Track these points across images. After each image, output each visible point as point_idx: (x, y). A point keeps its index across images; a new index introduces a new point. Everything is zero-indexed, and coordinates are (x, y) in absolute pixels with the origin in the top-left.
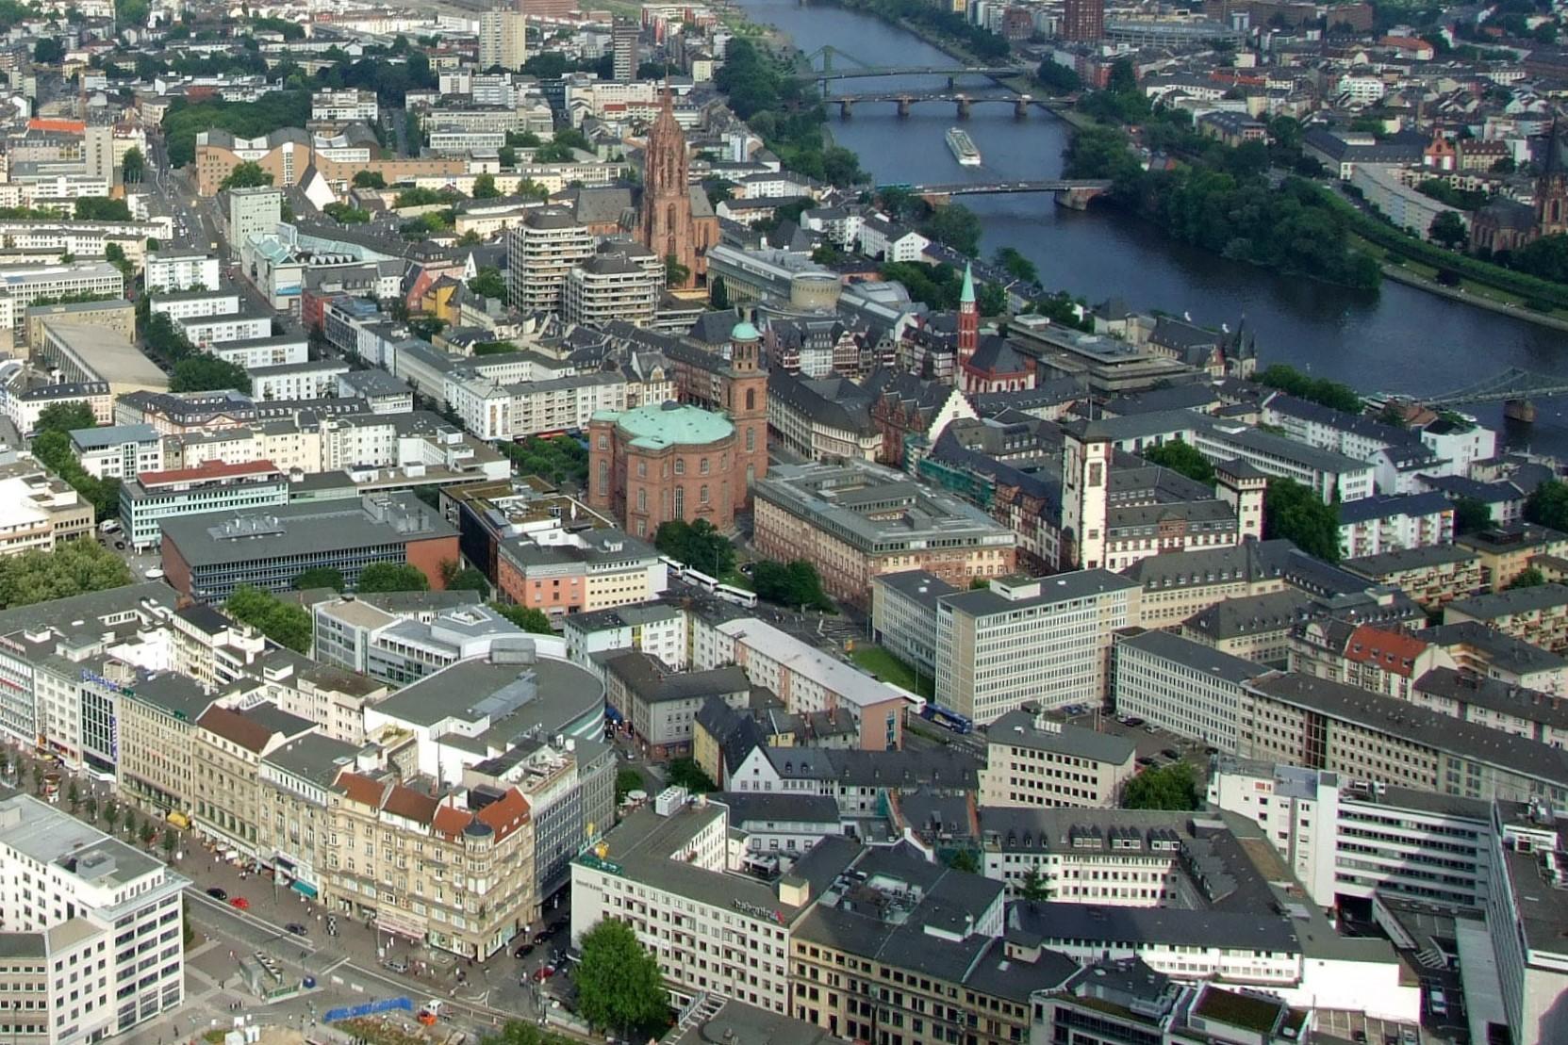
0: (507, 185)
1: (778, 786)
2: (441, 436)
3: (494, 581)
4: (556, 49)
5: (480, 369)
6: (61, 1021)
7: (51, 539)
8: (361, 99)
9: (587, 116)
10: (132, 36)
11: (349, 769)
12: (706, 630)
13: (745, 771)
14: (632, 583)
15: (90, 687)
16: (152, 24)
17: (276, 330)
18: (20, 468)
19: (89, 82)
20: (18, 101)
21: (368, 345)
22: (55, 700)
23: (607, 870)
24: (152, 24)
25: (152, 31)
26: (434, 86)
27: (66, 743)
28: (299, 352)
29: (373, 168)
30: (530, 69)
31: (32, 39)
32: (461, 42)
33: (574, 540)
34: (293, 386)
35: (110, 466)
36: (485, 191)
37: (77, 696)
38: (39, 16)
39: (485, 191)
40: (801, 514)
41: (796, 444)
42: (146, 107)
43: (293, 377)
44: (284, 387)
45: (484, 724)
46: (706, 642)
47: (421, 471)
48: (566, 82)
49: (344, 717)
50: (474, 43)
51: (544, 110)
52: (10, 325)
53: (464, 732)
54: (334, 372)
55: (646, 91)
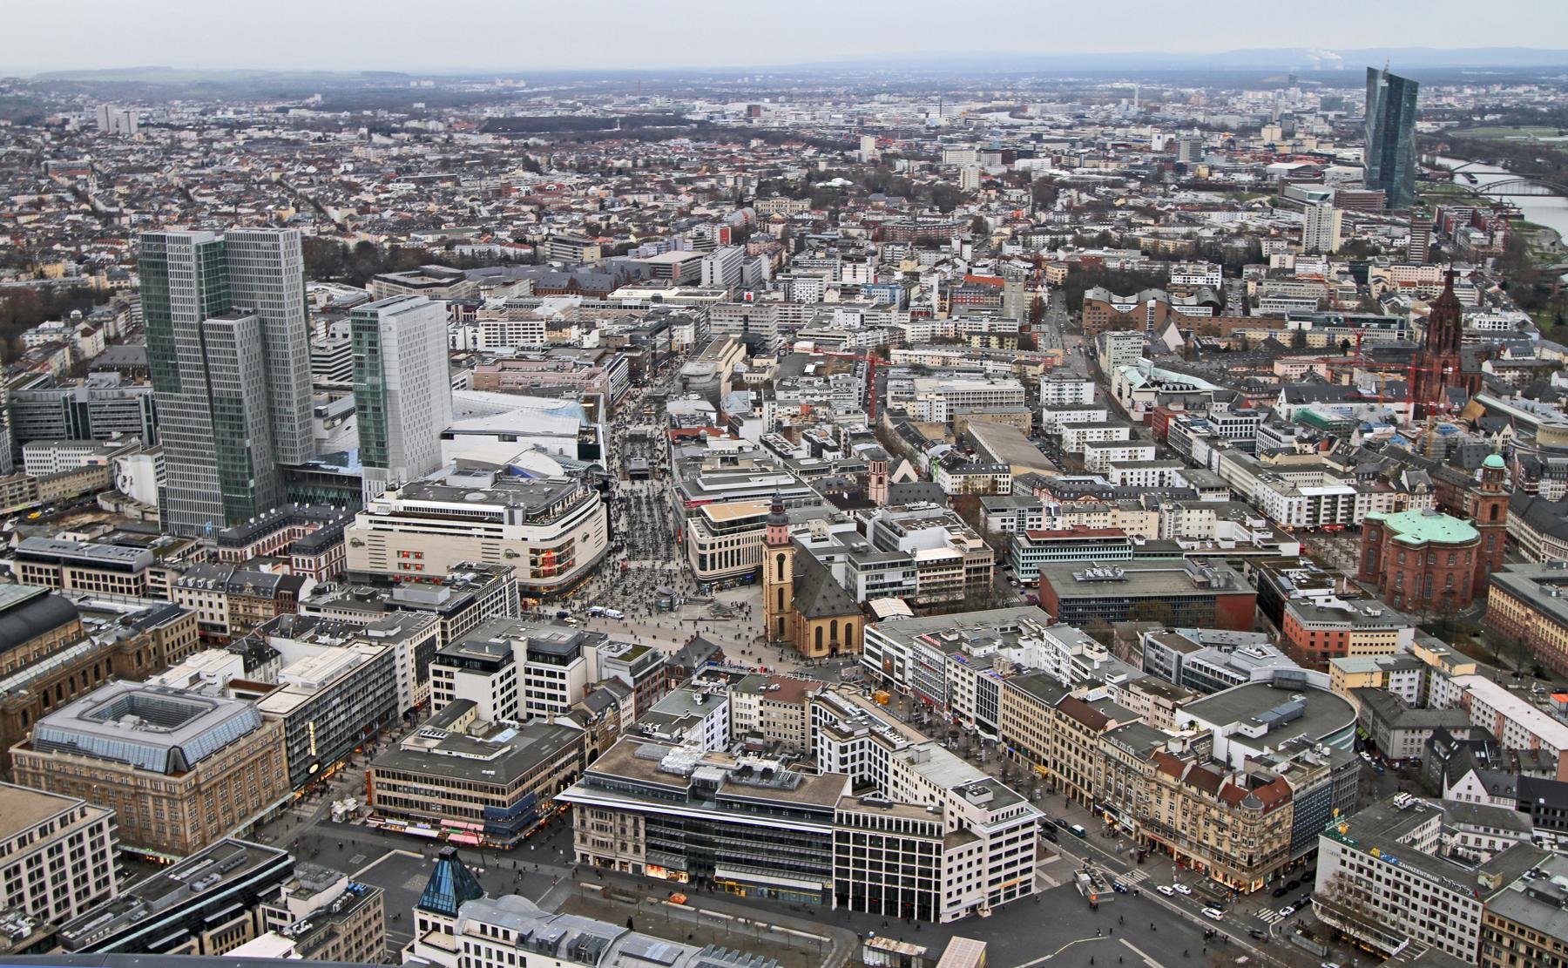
0: (1318, 339)
1: (1485, 800)
2: (1249, 521)
3: (1279, 626)
4: (1365, 238)
5: (1282, 474)
6: (949, 895)
7: (963, 571)
8: (1209, 270)
9: (1384, 289)
10: (1043, 216)
11: (1162, 750)
12: (1440, 680)
13: (1461, 786)
14: (1385, 640)
15: (985, 675)
16: (1059, 208)
17: (1134, 436)
18: (943, 520)
19: (1008, 250)
20: (957, 261)
21: (1200, 451)
22: (958, 680)
23: (1346, 843)
24: (1059, 208)
25: (1056, 213)
26: (1267, 261)
27: (964, 711)
28: (1148, 453)
29: (1215, 322)
30: (1344, 250)
31: (971, 216)
32: (1291, 231)
33: (1343, 605)
34: (1143, 477)
35: (1007, 524)
36: (1300, 344)
37: (974, 679)
38: (974, 199)
39: (1300, 344)
40: (1526, 601)
41: (1527, 550)
42: (1049, 269)
43: (1143, 471)
44: (1135, 477)
45: (1263, 729)
46: (1439, 688)
47: (1232, 545)
48: (1370, 263)
49: (1160, 713)
50: (1297, 230)
51: (1349, 283)
52: (944, 420)
53: (1248, 733)
54: (1173, 470)
55: (1435, 273)
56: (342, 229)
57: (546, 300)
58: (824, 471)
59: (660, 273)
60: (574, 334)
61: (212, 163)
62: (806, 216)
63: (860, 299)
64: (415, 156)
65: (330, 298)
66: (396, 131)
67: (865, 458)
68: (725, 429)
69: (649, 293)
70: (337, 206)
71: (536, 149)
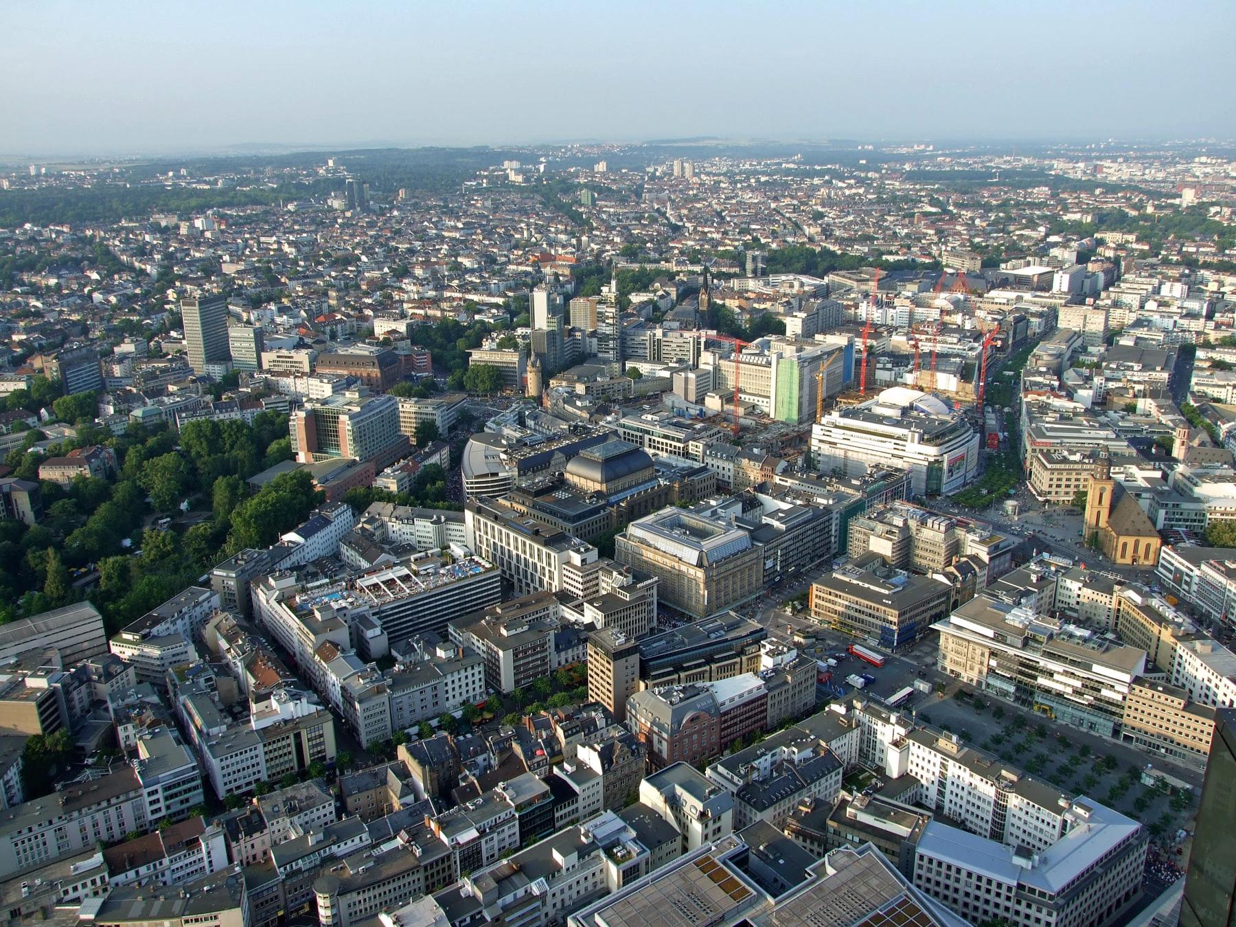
56: (811, 239)
57: (943, 295)
58: (1137, 431)
59: (1021, 283)
60: (958, 319)
61: (737, 196)
62: (1135, 246)
63: (1174, 309)
64: (860, 195)
65: (802, 284)
66: (849, 178)
67: (1171, 425)
68: (1064, 393)
69: (1012, 295)
70: (809, 225)
71: (937, 191)
